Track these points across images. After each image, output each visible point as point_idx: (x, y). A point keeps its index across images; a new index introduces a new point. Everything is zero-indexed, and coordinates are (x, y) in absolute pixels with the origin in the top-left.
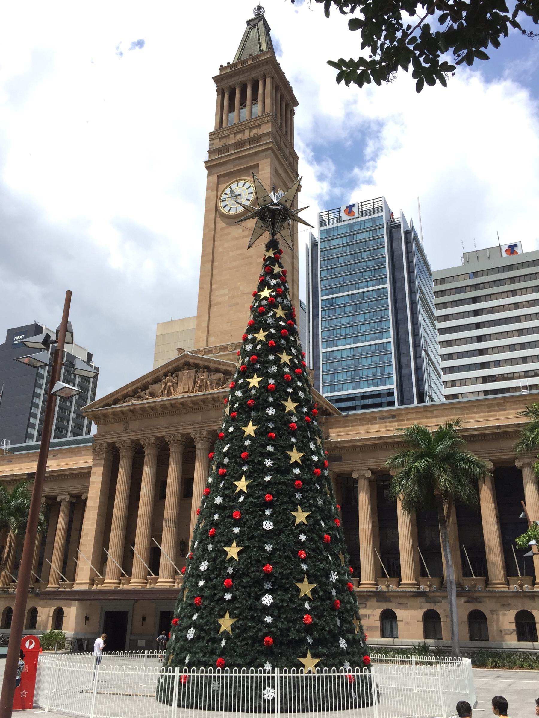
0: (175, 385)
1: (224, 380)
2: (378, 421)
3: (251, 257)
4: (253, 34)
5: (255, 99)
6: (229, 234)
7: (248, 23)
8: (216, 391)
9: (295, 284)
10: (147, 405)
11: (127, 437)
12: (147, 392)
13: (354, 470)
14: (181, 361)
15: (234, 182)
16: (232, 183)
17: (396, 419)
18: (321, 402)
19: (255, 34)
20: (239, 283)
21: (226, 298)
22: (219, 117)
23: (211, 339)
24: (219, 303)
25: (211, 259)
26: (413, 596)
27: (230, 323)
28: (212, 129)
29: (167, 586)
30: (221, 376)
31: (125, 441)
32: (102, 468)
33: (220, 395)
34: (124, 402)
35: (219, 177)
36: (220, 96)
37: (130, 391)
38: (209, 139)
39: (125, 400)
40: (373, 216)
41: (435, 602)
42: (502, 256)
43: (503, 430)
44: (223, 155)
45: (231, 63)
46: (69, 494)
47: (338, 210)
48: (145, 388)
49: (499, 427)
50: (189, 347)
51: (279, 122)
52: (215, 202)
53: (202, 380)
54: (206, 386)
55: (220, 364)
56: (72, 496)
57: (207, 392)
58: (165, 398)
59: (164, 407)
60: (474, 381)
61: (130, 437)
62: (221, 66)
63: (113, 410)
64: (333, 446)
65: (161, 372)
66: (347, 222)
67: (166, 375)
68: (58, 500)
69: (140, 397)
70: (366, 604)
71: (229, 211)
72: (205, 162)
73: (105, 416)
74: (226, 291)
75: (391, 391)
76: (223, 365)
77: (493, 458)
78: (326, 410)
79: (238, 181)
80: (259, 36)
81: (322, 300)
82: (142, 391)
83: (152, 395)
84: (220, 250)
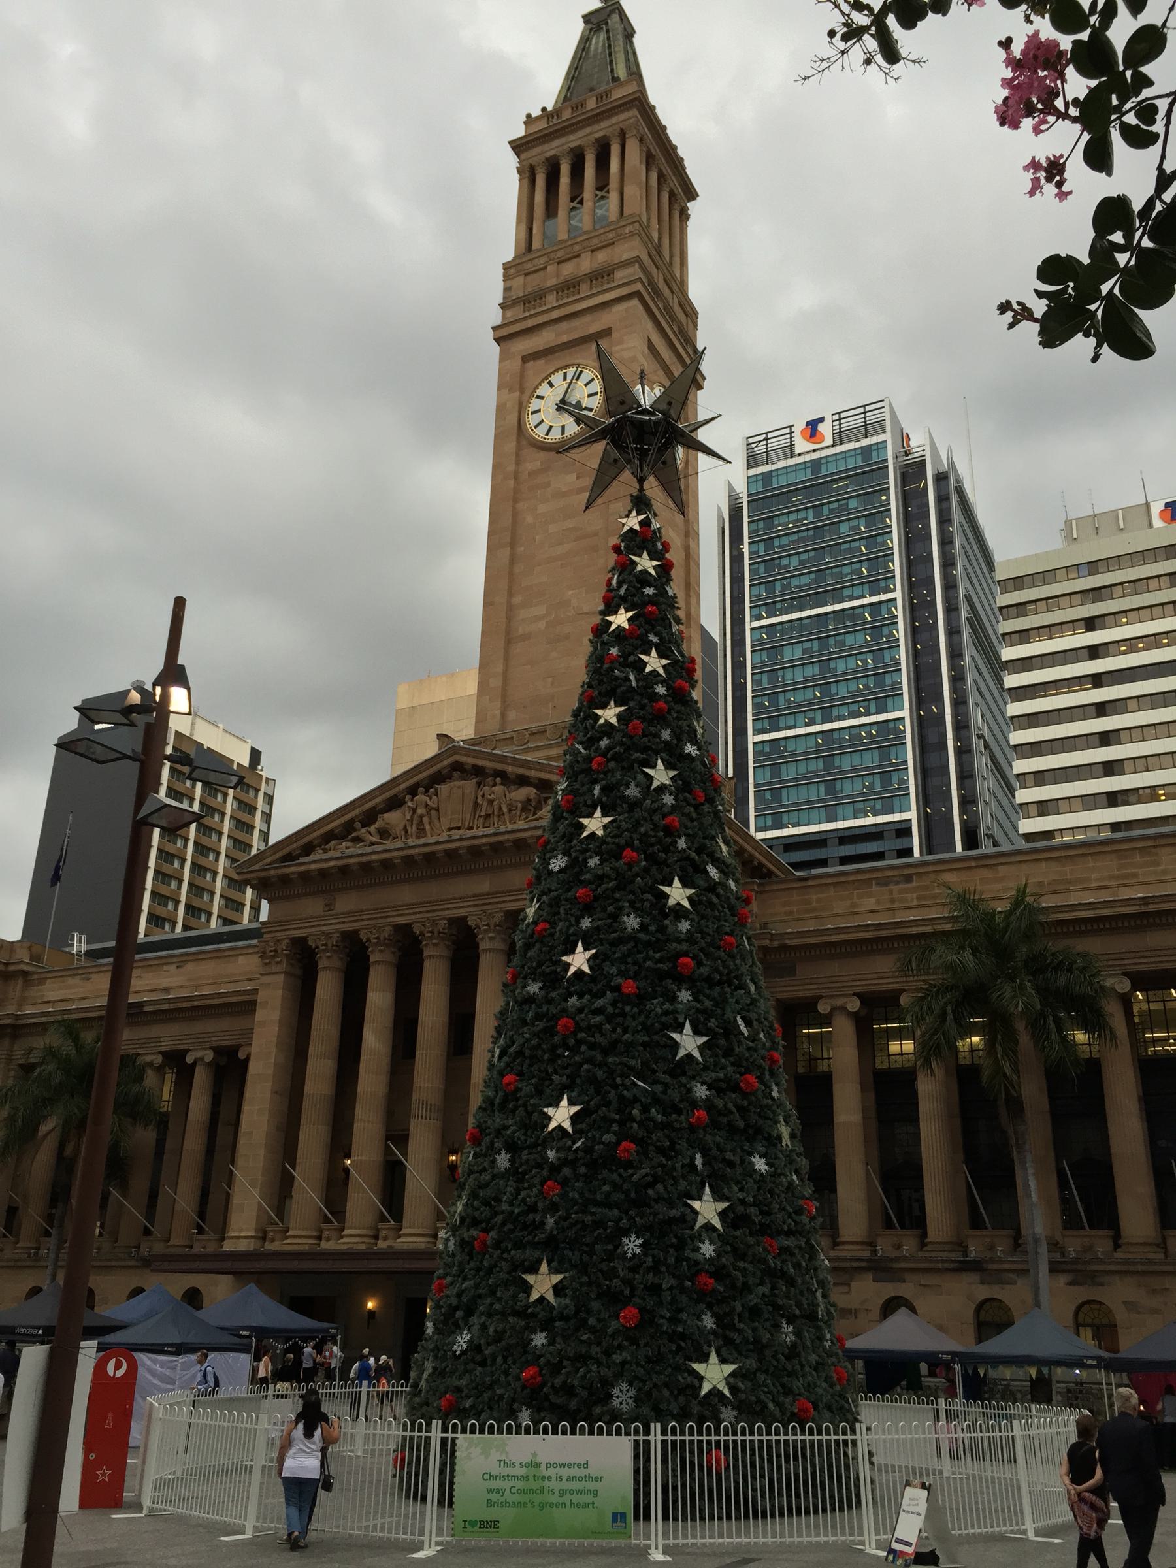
0: (433, 813)
1: (539, 802)
2: (875, 888)
3: (595, 534)
4: (597, 43)
5: (602, 185)
6: (548, 485)
7: (587, 18)
8: (521, 825)
9: (692, 593)
10: (374, 857)
11: (333, 927)
12: (373, 828)
13: (822, 997)
14: (445, 763)
15: (557, 371)
16: (553, 373)
17: (914, 884)
18: (749, 848)
19: (601, 44)
21: (542, 625)
22: (524, 227)
23: (512, 715)
24: (527, 637)
25: (508, 540)
26: (954, 1270)
28: (509, 255)
29: (421, 1243)
31: (328, 935)
32: (280, 992)
33: (529, 834)
34: (325, 851)
35: (525, 359)
36: (526, 181)
37: (336, 827)
38: (501, 278)
39: (328, 846)
40: (865, 442)
42: (1151, 525)
43: (1152, 907)
44: (532, 312)
45: (550, 109)
46: (211, 1048)
47: (788, 430)
48: (369, 818)
49: (1144, 901)
50: (463, 730)
51: (655, 235)
52: (516, 414)
53: (491, 802)
54: (501, 815)
55: (530, 768)
56: (217, 1051)
57: (502, 829)
58: (412, 842)
59: (409, 861)
60: (1090, 802)
61: (337, 927)
62: (529, 116)
63: (303, 868)
64: (776, 943)
65: (403, 786)
66: (808, 458)
67: (413, 791)
68: (189, 1059)
69: (358, 840)
70: (849, 1285)
71: (547, 434)
72: (494, 329)
73: (285, 880)
74: (541, 610)
75: (904, 825)
76: (537, 770)
77: (1130, 969)
78: (761, 865)
79: (565, 367)
80: (609, 46)
81: (752, 629)
82: (363, 827)
83: (384, 833)
84: (529, 519)
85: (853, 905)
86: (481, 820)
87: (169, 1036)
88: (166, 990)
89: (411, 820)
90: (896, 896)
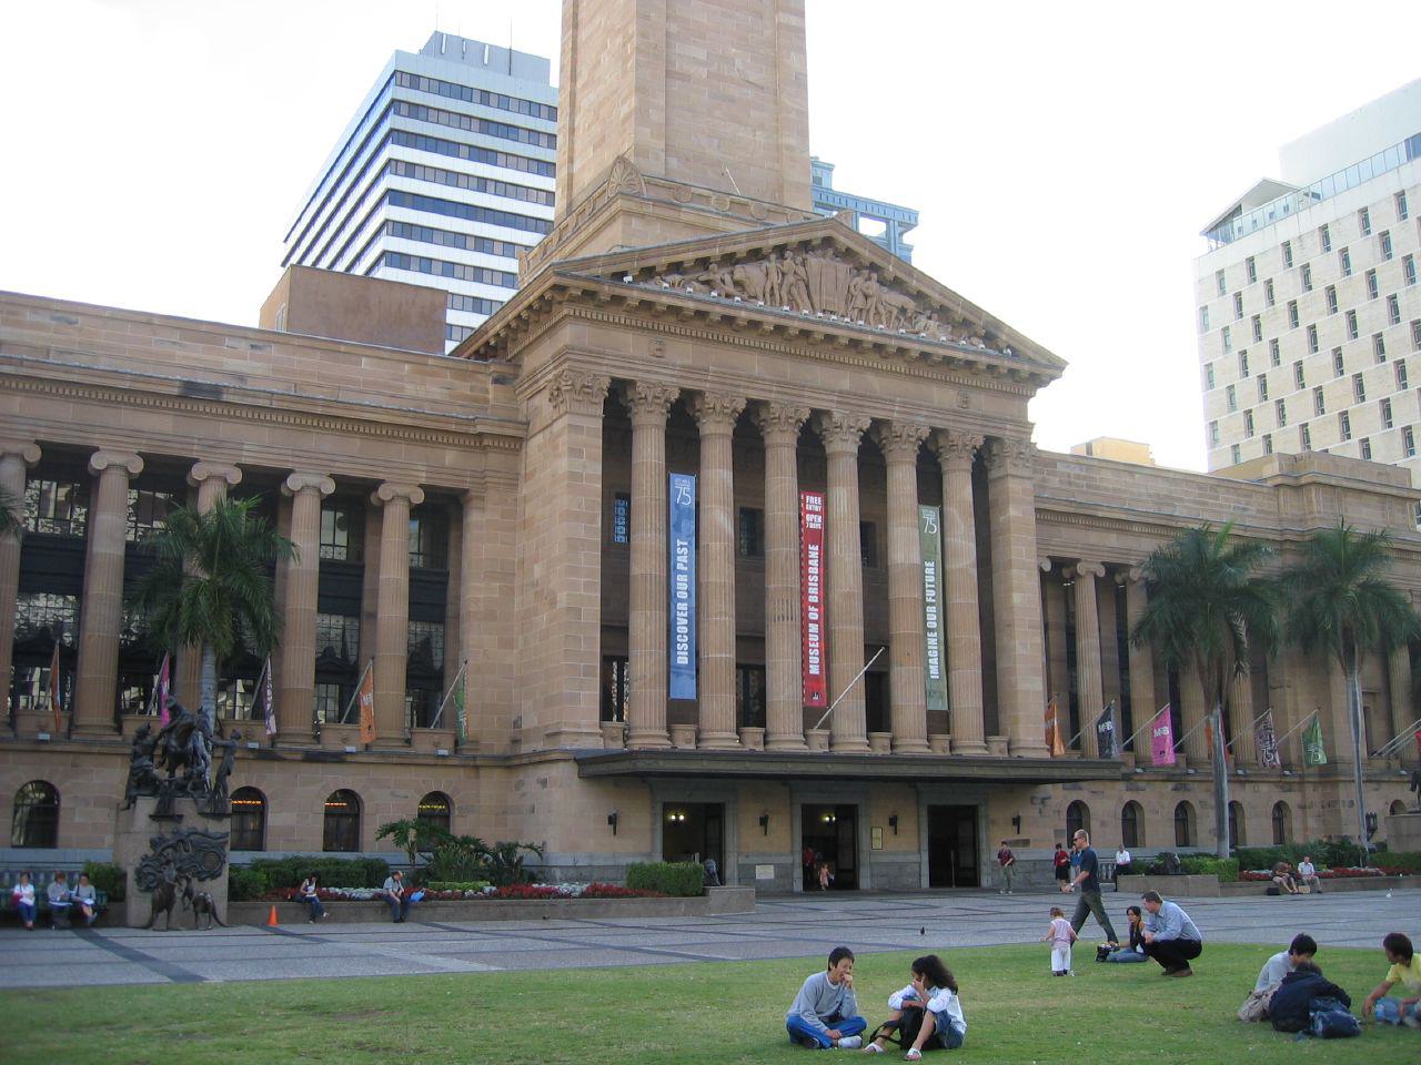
10: (743, 314)
11: (671, 383)
20: (734, 50)
21: (703, 72)
24: (685, 77)
27: (716, 141)
30: (911, 305)
41: (1138, 789)
56: (339, 480)
61: (674, 380)
65: (773, 242)
73: (618, 300)
76: (918, 280)
85: (1044, 480)
86: (856, 311)
87: (260, 446)
88: (241, 377)
89: (781, 285)
90: (1072, 480)
